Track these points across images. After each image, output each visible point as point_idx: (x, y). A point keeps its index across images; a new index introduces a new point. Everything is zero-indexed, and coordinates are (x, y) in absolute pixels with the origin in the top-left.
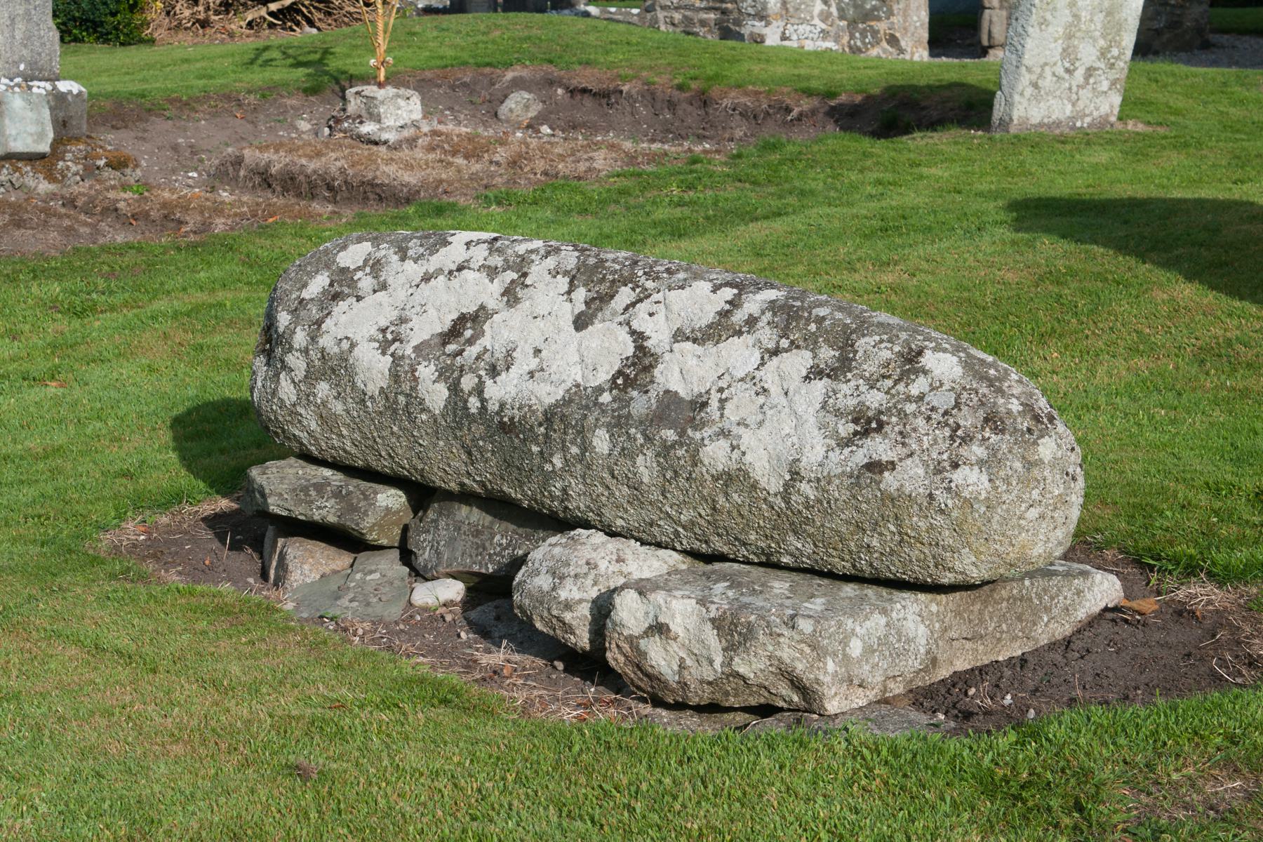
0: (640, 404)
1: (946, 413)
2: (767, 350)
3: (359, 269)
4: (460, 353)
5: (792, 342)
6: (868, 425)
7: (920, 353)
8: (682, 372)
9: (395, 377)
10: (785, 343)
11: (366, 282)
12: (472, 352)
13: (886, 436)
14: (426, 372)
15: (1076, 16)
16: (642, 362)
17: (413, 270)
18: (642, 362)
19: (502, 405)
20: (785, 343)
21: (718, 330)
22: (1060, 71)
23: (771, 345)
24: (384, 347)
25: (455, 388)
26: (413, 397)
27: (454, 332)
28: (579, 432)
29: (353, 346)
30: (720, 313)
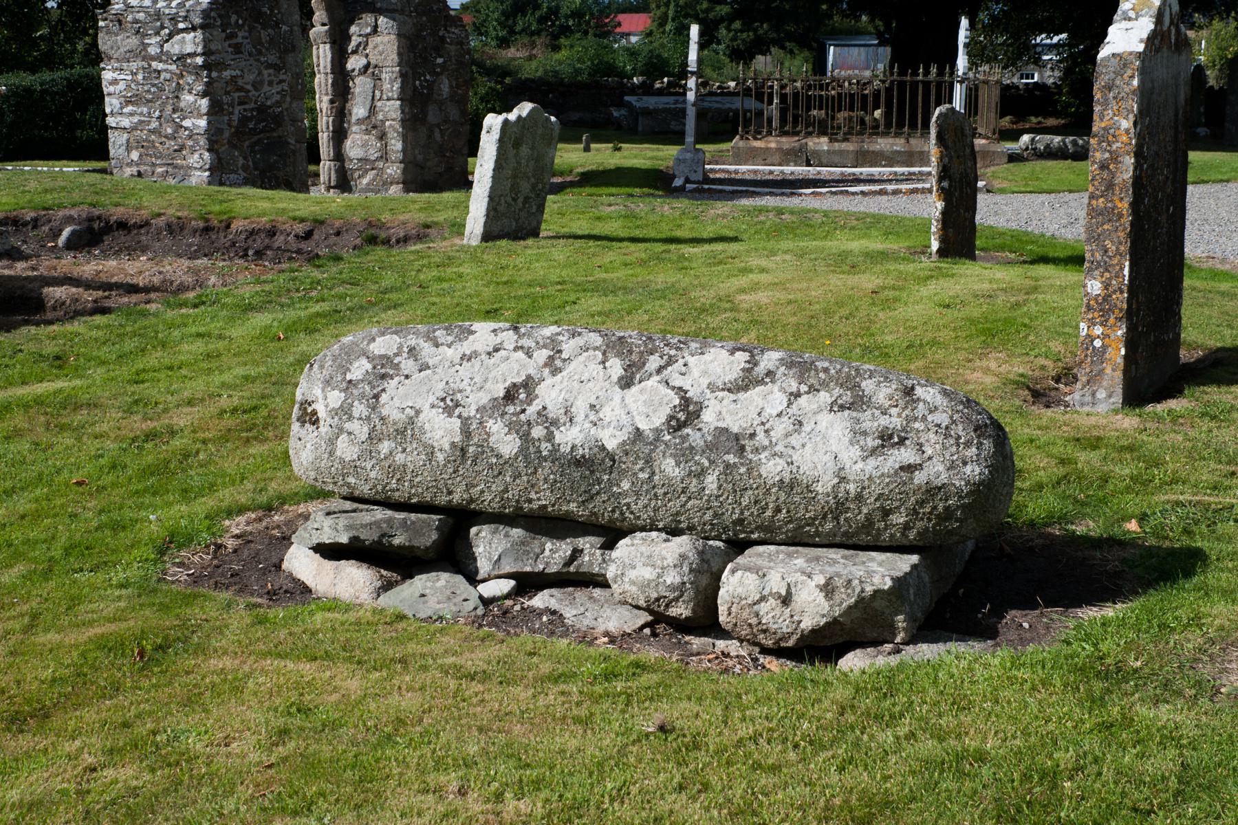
0: (694, 437)
1: (947, 428)
2: (791, 394)
3: (396, 355)
4: (523, 411)
5: (810, 387)
6: (888, 440)
7: (913, 388)
8: (720, 413)
9: (467, 433)
10: (804, 388)
11: (408, 365)
12: (532, 410)
13: (906, 447)
14: (496, 427)
15: (519, 163)
16: (687, 412)
17: (451, 353)
18: (687, 412)
19: (573, 447)
20: (804, 388)
21: (747, 381)
22: (509, 199)
23: (794, 389)
24: (449, 411)
25: (526, 437)
26: (485, 448)
27: (510, 396)
28: (647, 462)
29: (418, 412)
30: (743, 370)
